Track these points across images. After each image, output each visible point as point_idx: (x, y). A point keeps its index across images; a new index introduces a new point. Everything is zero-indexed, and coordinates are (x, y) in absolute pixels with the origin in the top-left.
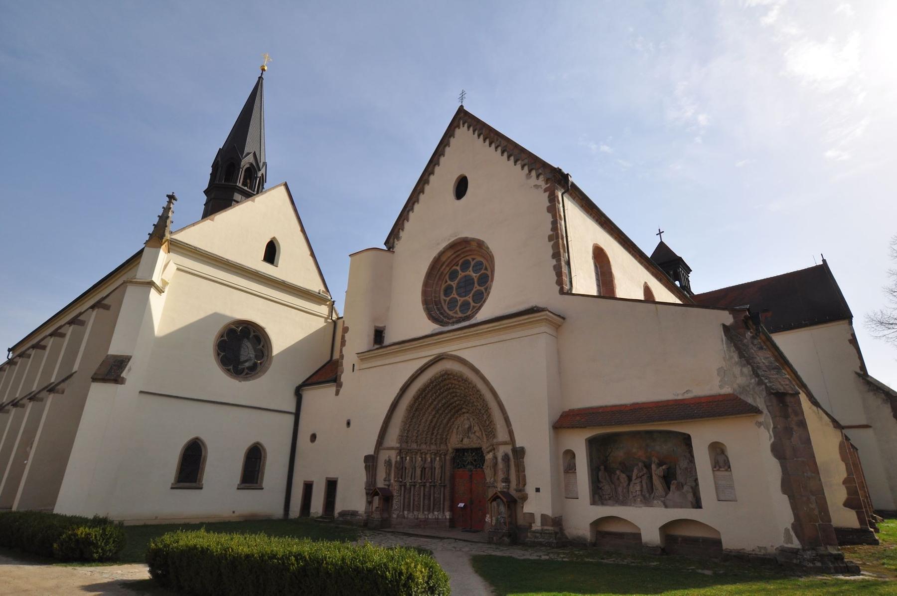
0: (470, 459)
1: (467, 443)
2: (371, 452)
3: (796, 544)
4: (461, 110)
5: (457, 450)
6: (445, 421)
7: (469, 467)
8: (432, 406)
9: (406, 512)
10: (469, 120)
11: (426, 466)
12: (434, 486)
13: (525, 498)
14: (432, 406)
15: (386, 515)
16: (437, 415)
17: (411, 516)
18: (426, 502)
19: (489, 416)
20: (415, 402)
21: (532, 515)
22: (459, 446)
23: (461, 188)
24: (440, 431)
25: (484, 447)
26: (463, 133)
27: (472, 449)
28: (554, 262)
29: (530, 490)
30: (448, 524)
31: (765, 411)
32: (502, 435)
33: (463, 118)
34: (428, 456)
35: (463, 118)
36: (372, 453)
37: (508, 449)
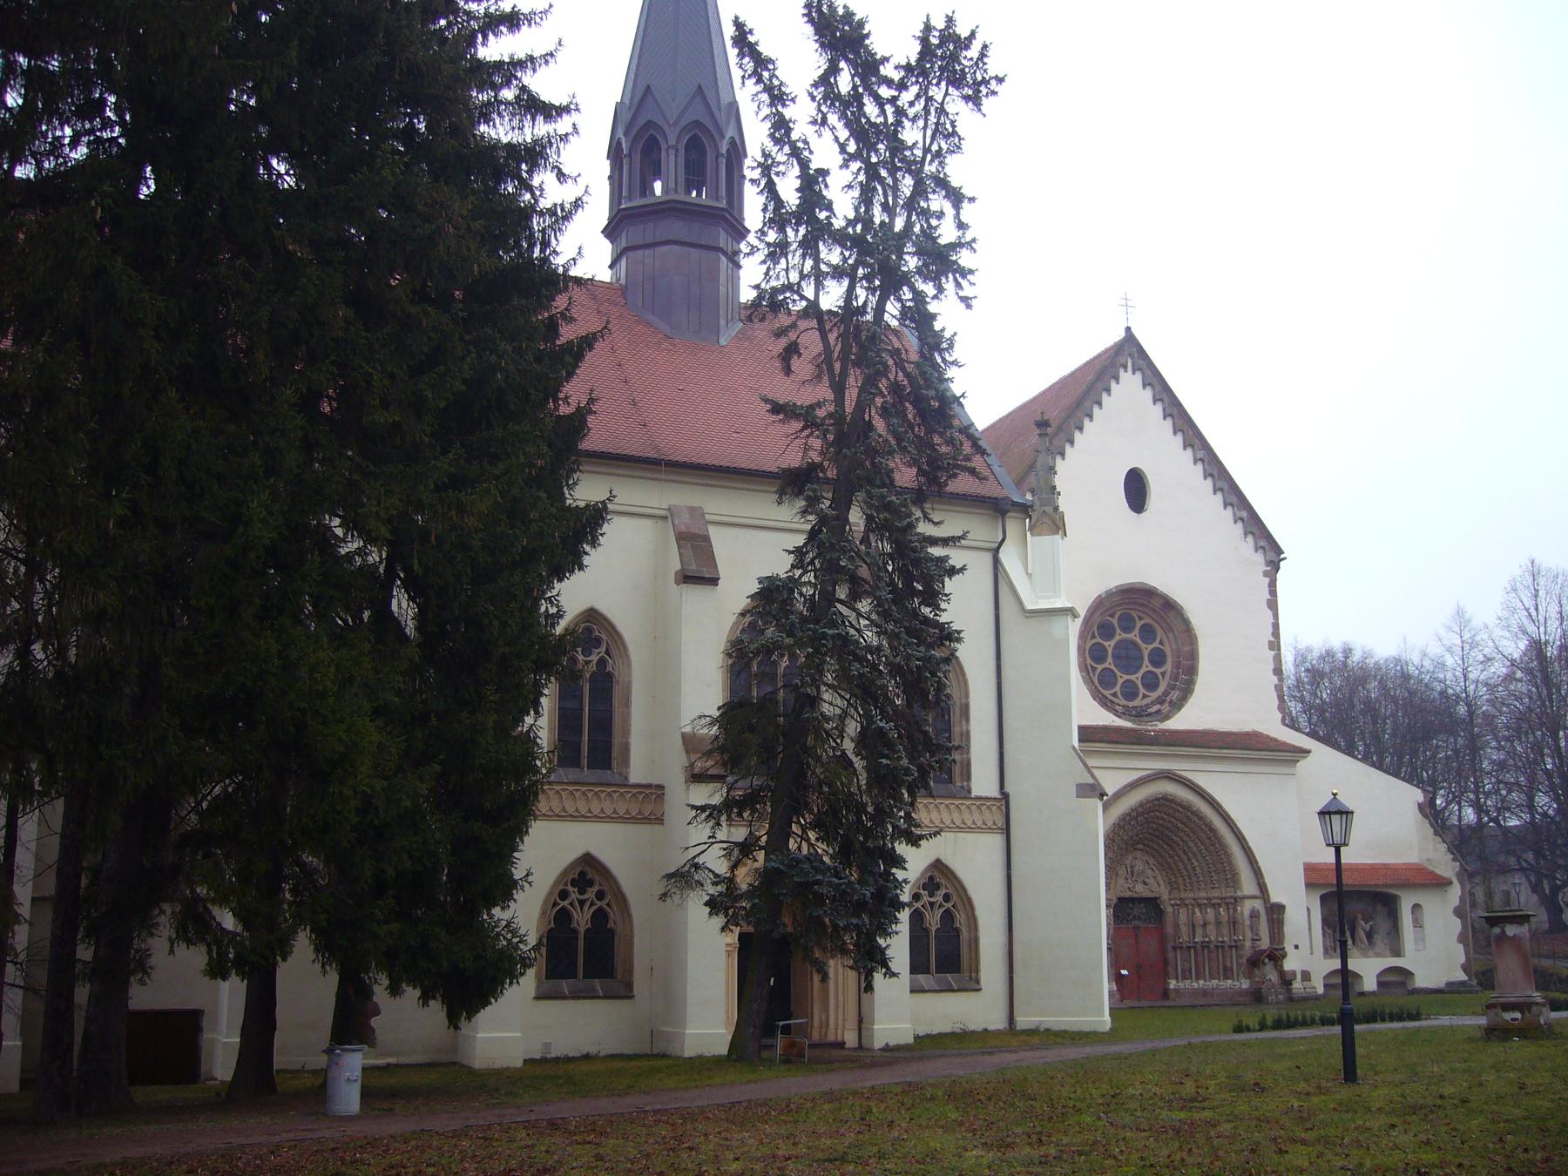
0: (1136, 912)
1: (1141, 890)
3: (1462, 977)
4: (1130, 339)
10: (1148, 372)
13: (1284, 956)
19: (1230, 863)
21: (1294, 973)
22: (1128, 894)
23: (1136, 489)
25: (1165, 897)
26: (1129, 384)
28: (1275, 680)
29: (1289, 947)
31: (1455, 881)
32: (1248, 886)
33: (1128, 354)
35: (1128, 354)
37: (1258, 905)
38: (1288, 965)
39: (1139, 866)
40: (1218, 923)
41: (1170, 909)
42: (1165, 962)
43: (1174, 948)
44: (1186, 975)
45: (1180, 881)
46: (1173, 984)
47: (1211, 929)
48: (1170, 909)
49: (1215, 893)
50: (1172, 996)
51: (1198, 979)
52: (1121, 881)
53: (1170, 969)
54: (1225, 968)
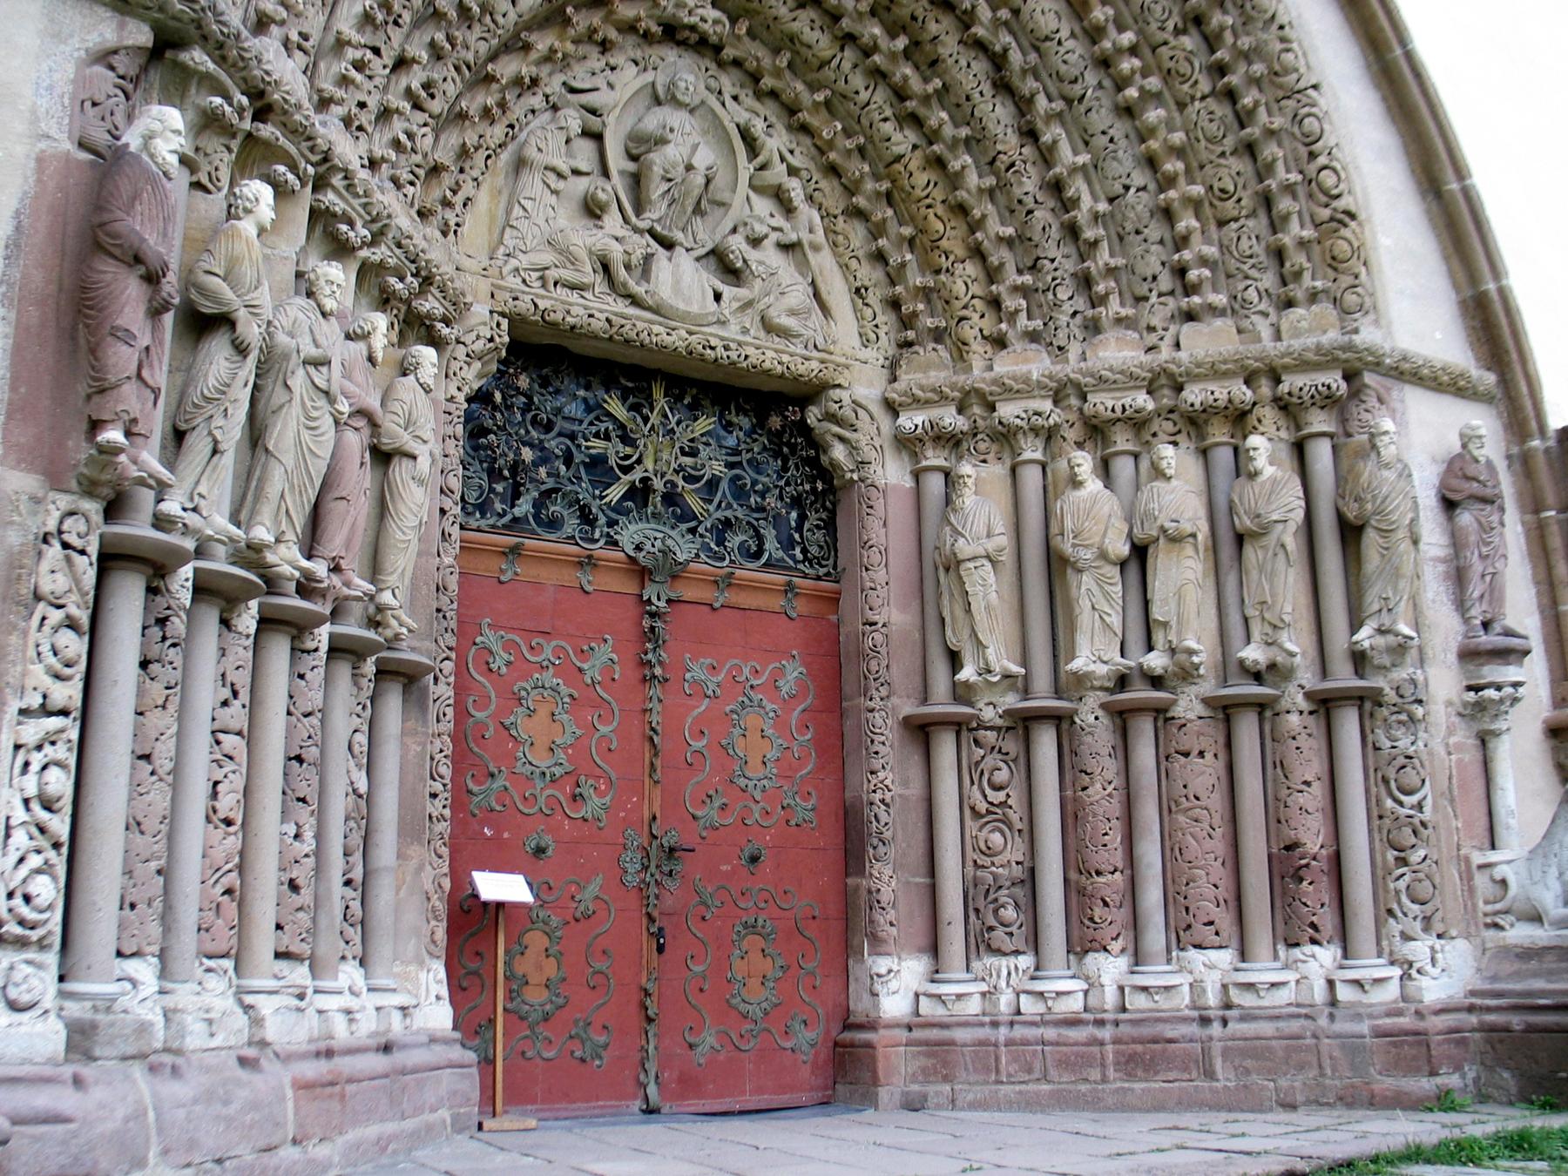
0: (657, 460)
7: (631, 533)
22: (593, 311)
25: (863, 384)
39: (688, 146)
40: (1234, 540)
41: (892, 473)
42: (852, 839)
43: (921, 731)
44: (998, 916)
45: (964, 280)
46: (897, 985)
47: (1181, 580)
48: (892, 473)
49: (1207, 342)
50: (898, 1066)
51: (1082, 945)
52: (547, 216)
53: (889, 879)
54: (1287, 865)
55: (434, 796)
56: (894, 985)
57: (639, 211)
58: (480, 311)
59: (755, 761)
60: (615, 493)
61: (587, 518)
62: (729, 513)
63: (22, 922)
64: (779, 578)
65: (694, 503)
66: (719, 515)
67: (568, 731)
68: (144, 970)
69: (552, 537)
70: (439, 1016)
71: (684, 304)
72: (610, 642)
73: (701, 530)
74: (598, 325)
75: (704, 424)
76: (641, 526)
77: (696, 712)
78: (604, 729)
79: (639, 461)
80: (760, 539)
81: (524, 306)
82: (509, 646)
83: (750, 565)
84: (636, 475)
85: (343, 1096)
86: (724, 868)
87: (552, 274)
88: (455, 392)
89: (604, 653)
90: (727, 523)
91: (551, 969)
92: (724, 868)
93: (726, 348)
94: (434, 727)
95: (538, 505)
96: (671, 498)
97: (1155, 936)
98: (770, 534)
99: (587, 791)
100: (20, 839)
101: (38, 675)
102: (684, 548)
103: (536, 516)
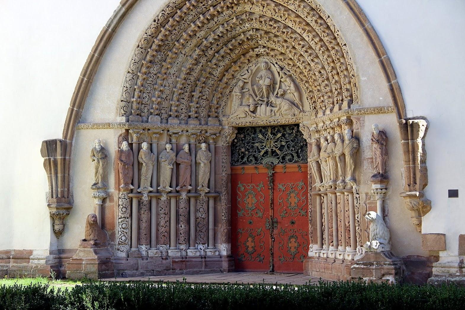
0: (270, 145)
2: (57, 133)
5: (240, 130)
6: (217, 73)
8: (194, 41)
9: (144, 247)
11: (180, 160)
12: (196, 198)
14: (194, 41)
15: (104, 254)
16: (203, 61)
17: (152, 252)
18: (183, 226)
20: (157, 30)
24: (207, 91)
27: (273, 127)
30: (225, 265)
34: (183, 139)
36: (58, 134)
38: (431, 224)
55: (223, 216)
56: (311, 250)
57: (257, 97)
58: (227, 127)
59: (293, 203)
60: (262, 153)
61: (256, 159)
62: (286, 153)
63: (121, 242)
64: (296, 165)
65: (278, 152)
66: (284, 153)
67: (255, 201)
68: (144, 247)
69: (250, 164)
70: (224, 253)
71: (264, 116)
72: (262, 183)
73: (280, 158)
74: (248, 124)
75: (279, 135)
76: (267, 159)
77: (280, 195)
78: (262, 200)
79: (265, 146)
80: (293, 157)
81: (234, 125)
82: (244, 186)
83: (290, 163)
84: (265, 149)
85: (186, 264)
86: (286, 225)
87: (239, 116)
88: (223, 144)
89: (261, 185)
90: (286, 155)
91: (253, 244)
92: (286, 225)
93: (275, 121)
94: (223, 204)
95: (248, 159)
96: (273, 152)
97: (335, 243)
98: (295, 155)
99: (258, 211)
100: (120, 233)
101: (120, 214)
102: (276, 161)
103: (248, 161)
